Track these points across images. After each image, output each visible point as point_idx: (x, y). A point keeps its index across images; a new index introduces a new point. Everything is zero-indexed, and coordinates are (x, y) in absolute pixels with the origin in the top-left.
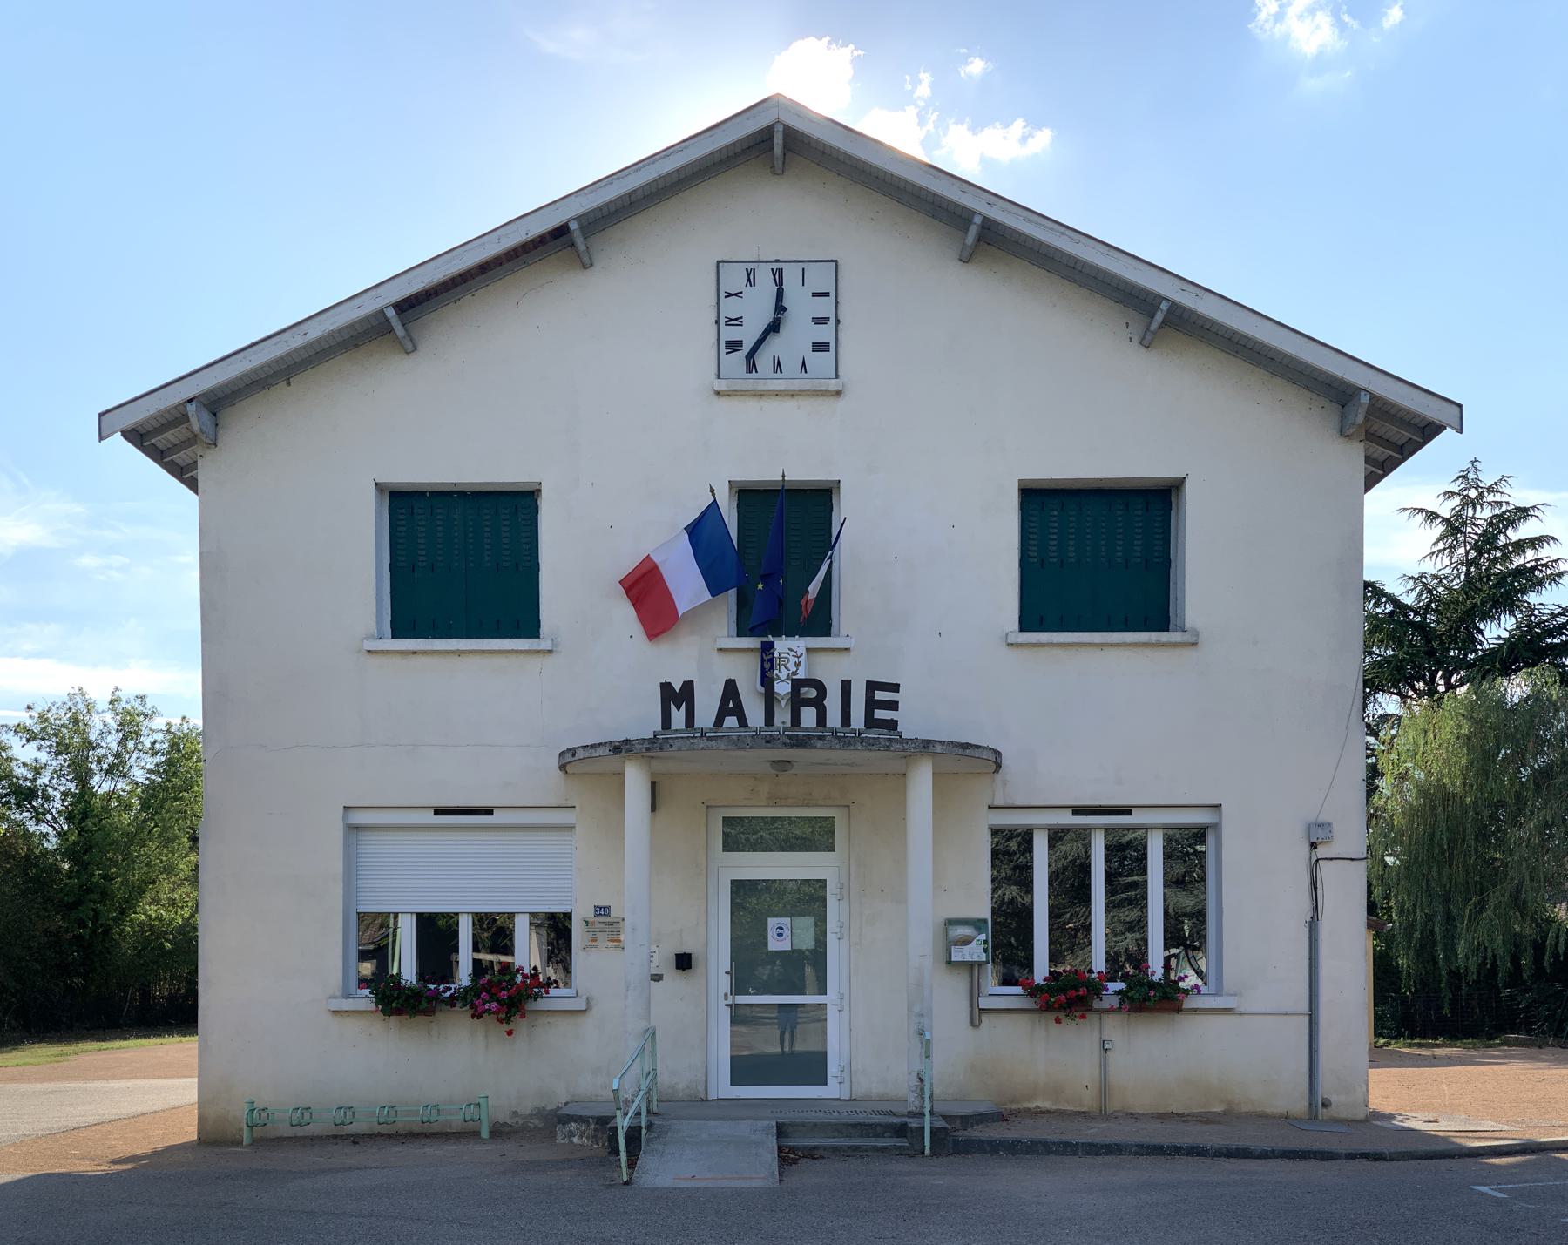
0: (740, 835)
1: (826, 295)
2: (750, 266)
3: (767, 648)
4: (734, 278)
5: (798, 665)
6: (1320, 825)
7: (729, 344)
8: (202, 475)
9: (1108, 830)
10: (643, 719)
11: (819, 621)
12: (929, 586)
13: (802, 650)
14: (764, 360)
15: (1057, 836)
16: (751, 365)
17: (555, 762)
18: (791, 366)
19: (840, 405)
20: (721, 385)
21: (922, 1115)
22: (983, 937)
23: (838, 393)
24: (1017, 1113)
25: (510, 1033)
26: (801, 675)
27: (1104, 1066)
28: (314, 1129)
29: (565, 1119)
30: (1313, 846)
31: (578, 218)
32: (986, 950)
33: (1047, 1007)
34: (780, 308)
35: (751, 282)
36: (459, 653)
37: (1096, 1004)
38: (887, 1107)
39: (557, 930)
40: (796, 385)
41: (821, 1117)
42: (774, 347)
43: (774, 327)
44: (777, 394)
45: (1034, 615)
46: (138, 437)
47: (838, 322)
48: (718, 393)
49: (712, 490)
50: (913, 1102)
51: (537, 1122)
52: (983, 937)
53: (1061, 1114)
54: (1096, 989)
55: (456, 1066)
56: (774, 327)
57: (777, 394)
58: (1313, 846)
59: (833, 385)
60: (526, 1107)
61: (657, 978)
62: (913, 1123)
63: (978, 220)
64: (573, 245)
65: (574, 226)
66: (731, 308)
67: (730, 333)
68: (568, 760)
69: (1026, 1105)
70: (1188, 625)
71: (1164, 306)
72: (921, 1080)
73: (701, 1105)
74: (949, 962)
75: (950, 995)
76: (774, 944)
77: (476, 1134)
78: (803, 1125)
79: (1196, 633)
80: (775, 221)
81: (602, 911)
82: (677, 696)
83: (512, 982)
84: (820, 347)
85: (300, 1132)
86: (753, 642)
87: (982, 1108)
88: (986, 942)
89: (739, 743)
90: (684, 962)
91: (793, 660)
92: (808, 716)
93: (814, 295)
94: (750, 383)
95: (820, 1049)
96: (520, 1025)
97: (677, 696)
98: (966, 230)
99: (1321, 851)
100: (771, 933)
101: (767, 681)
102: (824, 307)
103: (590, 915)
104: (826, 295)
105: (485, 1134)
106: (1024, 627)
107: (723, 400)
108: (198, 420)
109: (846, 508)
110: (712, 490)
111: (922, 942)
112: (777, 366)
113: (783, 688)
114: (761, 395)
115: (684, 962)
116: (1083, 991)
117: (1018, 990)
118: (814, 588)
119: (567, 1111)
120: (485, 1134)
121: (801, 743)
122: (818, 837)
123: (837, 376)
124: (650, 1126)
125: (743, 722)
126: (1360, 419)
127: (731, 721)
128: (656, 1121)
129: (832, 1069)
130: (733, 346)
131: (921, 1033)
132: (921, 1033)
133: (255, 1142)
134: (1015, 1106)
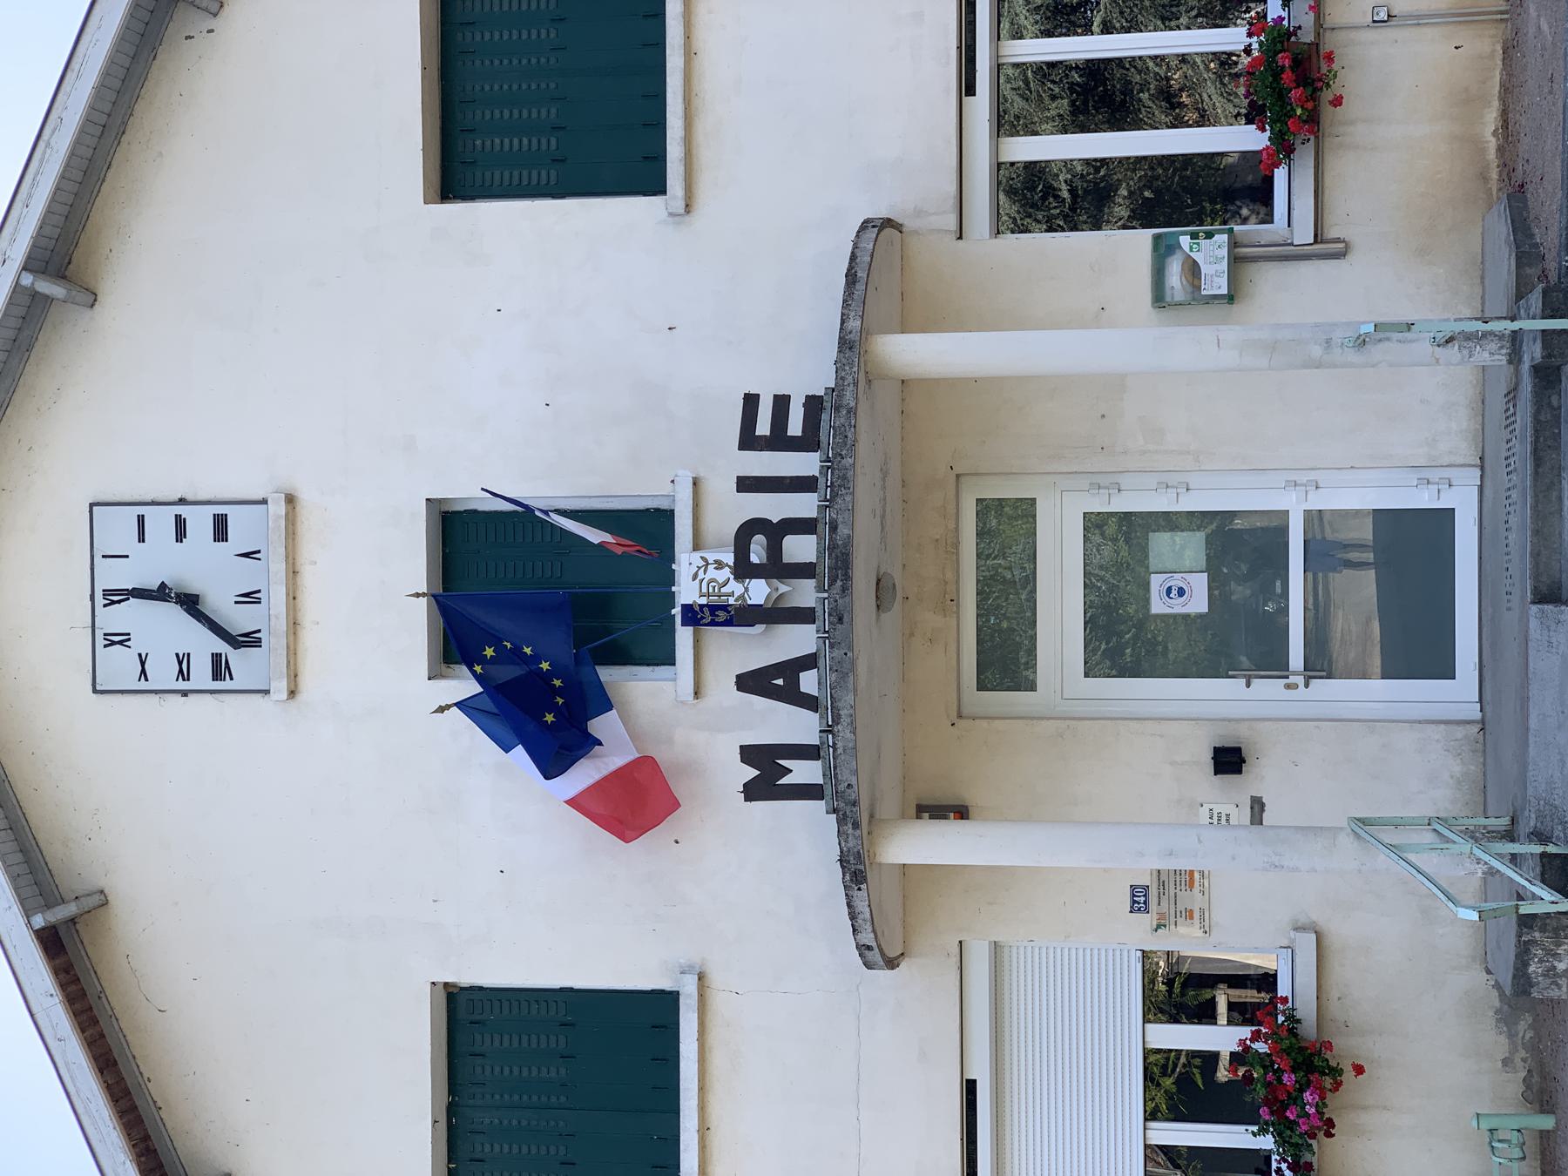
0: (1006, 660)
1: (141, 520)
2: (100, 642)
3: (692, 615)
4: (119, 666)
5: (720, 565)
7: (217, 676)
9: (997, 37)
11: (648, 530)
12: (598, 351)
13: (696, 558)
14: (241, 619)
15: (1006, 123)
16: (249, 640)
17: (884, 975)
18: (247, 576)
19: (308, 497)
20: (280, 687)
21: (1516, 336)
22: (1185, 241)
23: (290, 500)
24: (1507, 169)
25: (1359, 1070)
26: (729, 558)
27: (1418, 20)
32: (1209, 235)
33: (1313, 121)
34: (161, 593)
35: (124, 640)
36: (704, 1130)
37: (1307, 37)
38: (1497, 401)
39: (1180, 992)
40: (278, 567)
41: (1520, 519)
42: (220, 602)
43: (190, 603)
44: (292, 597)
45: (638, 170)
47: (182, 501)
48: (292, 693)
49: (441, 709)
50: (1492, 356)
51: (1522, 1026)
52: (1185, 241)
53: (1506, 90)
54: (1279, 38)
56: (190, 603)
57: (292, 597)
59: (277, 508)
60: (1498, 1044)
61: (1258, 806)
62: (1533, 352)
64: (73, 921)
66: (163, 673)
68: (880, 954)
69: (1492, 154)
72: (1450, 340)
73: (1495, 732)
74: (1230, 298)
75: (1292, 296)
76: (1198, 602)
78: (1536, 555)
81: (1139, 900)
83: (1265, 1061)
84: (221, 529)
86: (684, 636)
87: (1501, 228)
88: (1194, 236)
89: (843, 671)
90: (1229, 760)
92: (800, 548)
93: (142, 539)
94: (275, 642)
95: (1369, 521)
96: (1345, 1049)
98: (48, 300)
100: (1177, 607)
102: (160, 523)
103: (1146, 920)
104: (141, 520)
105: (1547, 1122)
106: (660, 189)
107: (307, 682)
109: (468, 488)
110: (441, 709)
111: (1196, 345)
112: (251, 597)
113: (759, 592)
114: (294, 625)
115: (1229, 760)
116: (1284, 60)
117: (1280, 175)
118: (594, 536)
120: (1547, 1122)
121: (839, 563)
122: (1007, 527)
123: (264, 502)
125: (809, 662)
129: (1424, 499)
130: (220, 668)
131: (1362, 342)
132: (1362, 342)
134: (1494, 175)
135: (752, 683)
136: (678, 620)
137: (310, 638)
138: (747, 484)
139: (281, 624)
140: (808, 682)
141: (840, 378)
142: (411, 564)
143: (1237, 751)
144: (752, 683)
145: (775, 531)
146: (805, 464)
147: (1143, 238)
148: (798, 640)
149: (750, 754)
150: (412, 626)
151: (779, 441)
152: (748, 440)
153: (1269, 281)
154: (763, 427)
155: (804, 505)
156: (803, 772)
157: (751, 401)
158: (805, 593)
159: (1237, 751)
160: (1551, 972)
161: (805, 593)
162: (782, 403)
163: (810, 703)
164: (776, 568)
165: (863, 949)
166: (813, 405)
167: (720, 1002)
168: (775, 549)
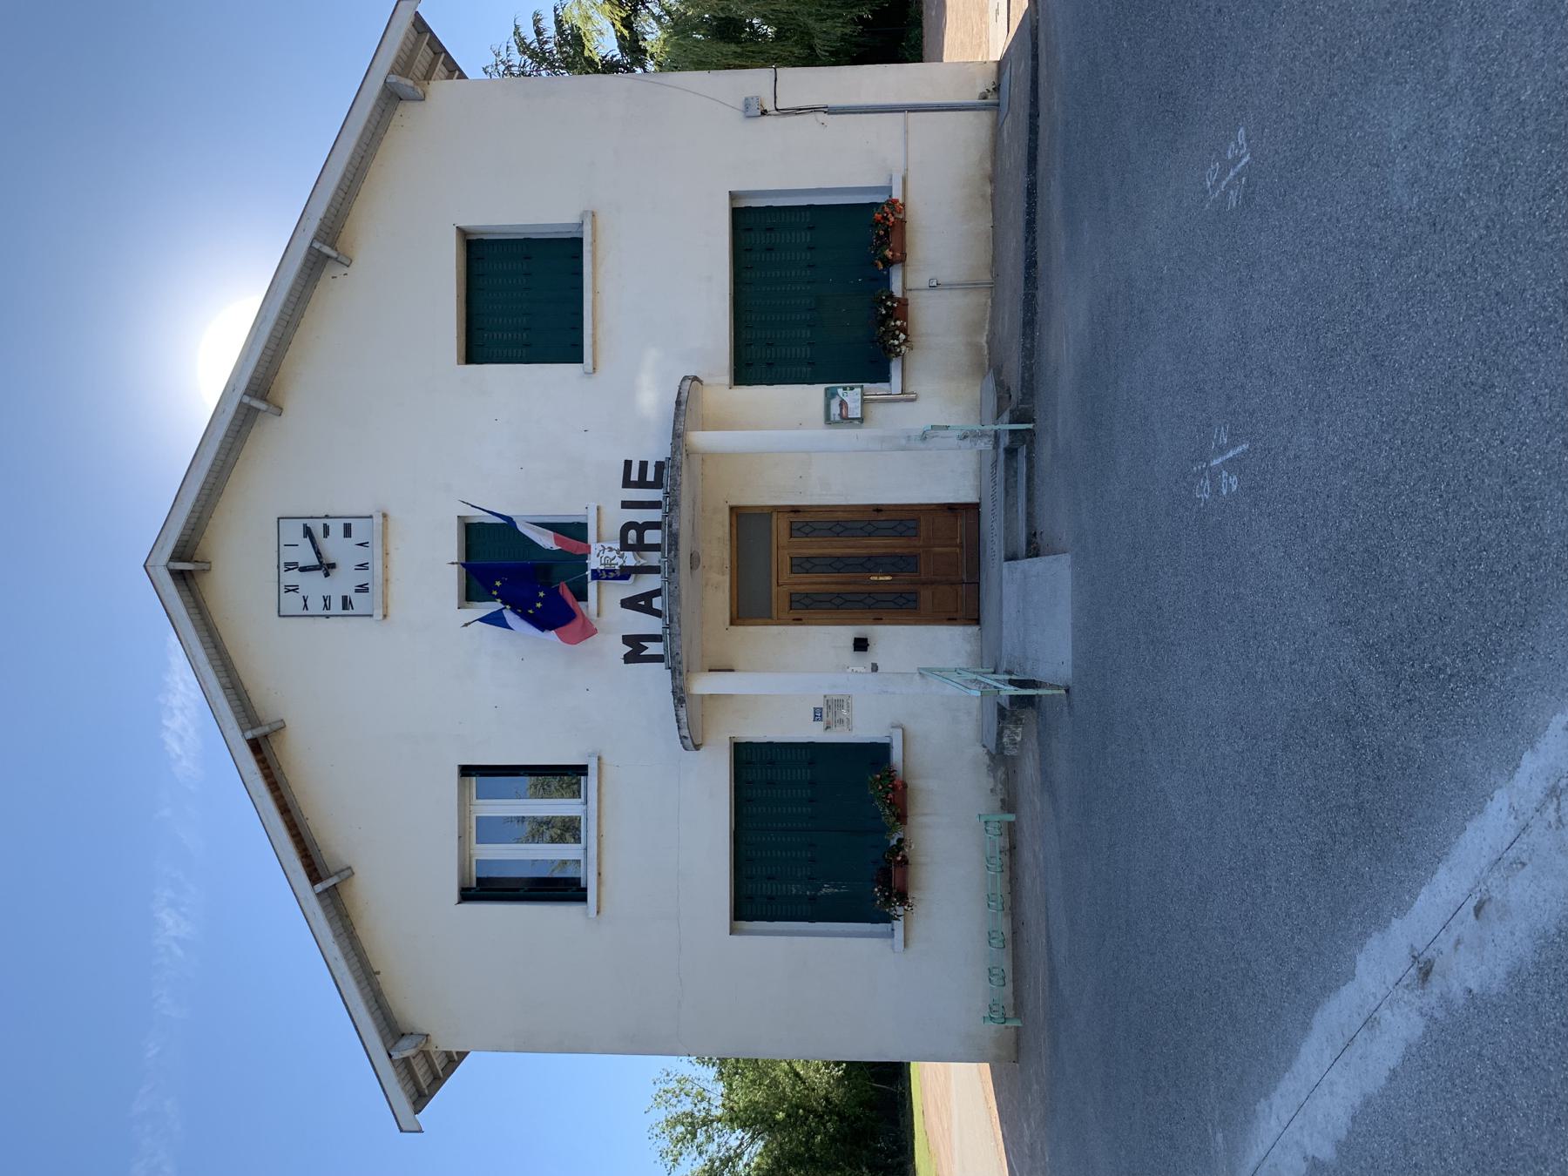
2: (283, 590)
3: (597, 575)
4: (292, 602)
5: (611, 549)
6: (747, 107)
10: (657, 674)
11: (574, 531)
12: (549, 444)
17: (693, 754)
18: (362, 556)
19: (393, 514)
20: (378, 613)
22: (840, 391)
23: (385, 516)
26: (617, 546)
27: (951, 286)
28: (1007, 965)
29: (1000, 745)
30: (764, 113)
31: (243, 732)
35: (295, 589)
36: (600, 836)
38: (988, 469)
40: (378, 551)
44: (385, 567)
45: (570, 351)
46: (420, 1099)
47: (327, 517)
51: (1000, 773)
55: (949, 840)
57: (385, 567)
58: (764, 113)
59: (378, 520)
60: (988, 783)
61: (875, 668)
63: (246, 399)
65: (249, 735)
66: (316, 606)
67: (336, 606)
70: (577, 220)
71: (317, 245)
77: (1011, 825)
79: (583, 214)
80: (245, 569)
81: (818, 715)
82: (636, 649)
84: (347, 531)
85: (1009, 976)
86: (592, 587)
89: (675, 598)
91: (607, 553)
92: (652, 537)
94: (376, 589)
99: (769, 107)
101: (625, 573)
103: (821, 725)
105: (1011, 818)
106: (579, 359)
107: (391, 611)
108: (406, 1049)
113: (630, 559)
119: (992, 746)
120: (1011, 818)
121: (673, 539)
124: (1009, 672)
125: (657, 593)
126: (410, 83)
127: (657, 603)
128: (1005, 666)
133: (1017, 1015)
135: (628, 603)
137: (392, 588)
138: (626, 505)
139: (379, 580)
140: (657, 603)
141: (674, 453)
142: (450, 548)
143: (865, 640)
144: (628, 603)
145: (641, 528)
147: (819, 390)
148: (650, 583)
149: (627, 640)
150: (450, 579)
151: (642, 483)
152: (627, 483)
153: (878, 411)
154: (634, 477)
155: (655, 515)
156: (653, 648)
157: (628, 464)
158: (653, 558)
159: (865, 640)
160: (1014, 742)
161: (653, 558)
162: (644, 465)
163: (658, 613)
164: (640, 547)
165: (683, 738)
166: (660, 466)
167: (607, 770)
168: (640, 537)
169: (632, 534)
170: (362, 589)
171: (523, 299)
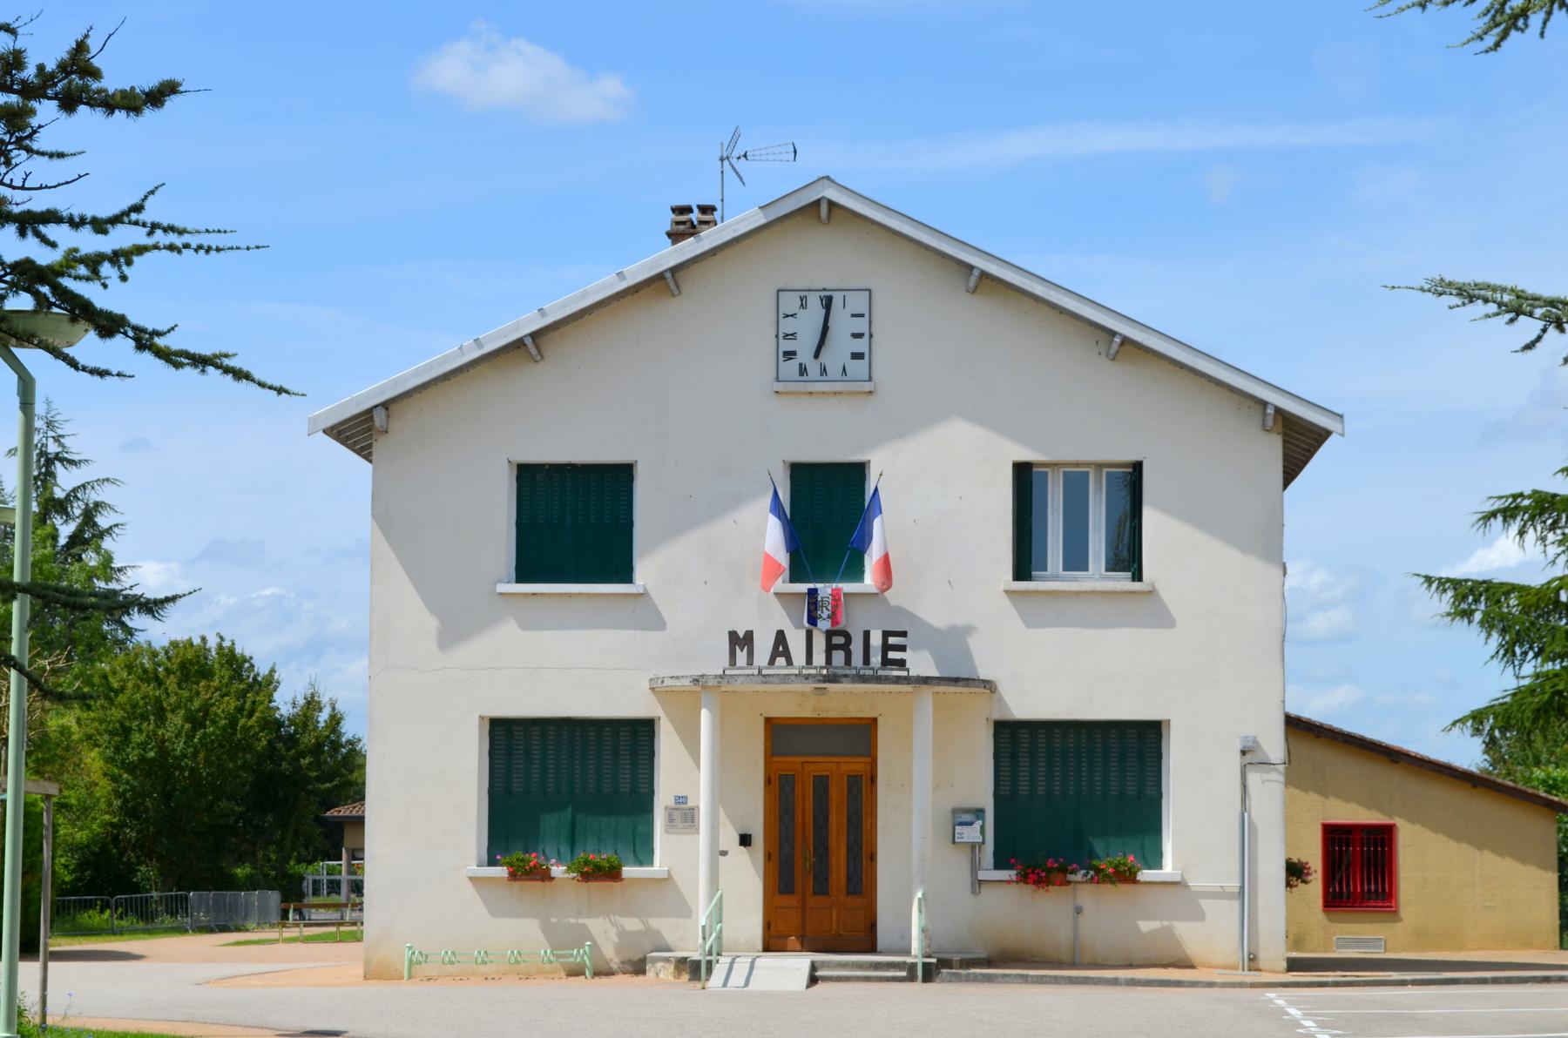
1: (862, 315)
3: (812, 593)
4: (790, 303)
8: (374, 457)
18: (834, 371)
20: (780, 387)
27: (1076, 927)
40: (838, 387)
59: (867, 386)
66: (787, 326)
67: (787, 345)
81: (681, 800)
84: (857, 356)
86: (803, 588)
92: (838, 657)
97: (741, 641)
99: (1248, 758)
102: (861, 325)
103: (671, 803)
104: (862, 315)
121: (833, 679)
123: (870, 379)
125: (789, 662)
127: (781, 661)
130: (790, 355)
135: (780, 637)
136: (811, 586)
139: (811, 387)
144: (780, 637)
145: (846, 647)
146: (876, 659)
148: (799, 656)
149: (749, 635)
151: (886, 647)
154: (892, 640)
157: (904, 634)
158: (819, 658)
163: (772, 662)
164: (830, 648)
166: (901, 664)
168: (838, 647)
169: (840, 640)
170: (803, 370)
171: (1077, 521)
